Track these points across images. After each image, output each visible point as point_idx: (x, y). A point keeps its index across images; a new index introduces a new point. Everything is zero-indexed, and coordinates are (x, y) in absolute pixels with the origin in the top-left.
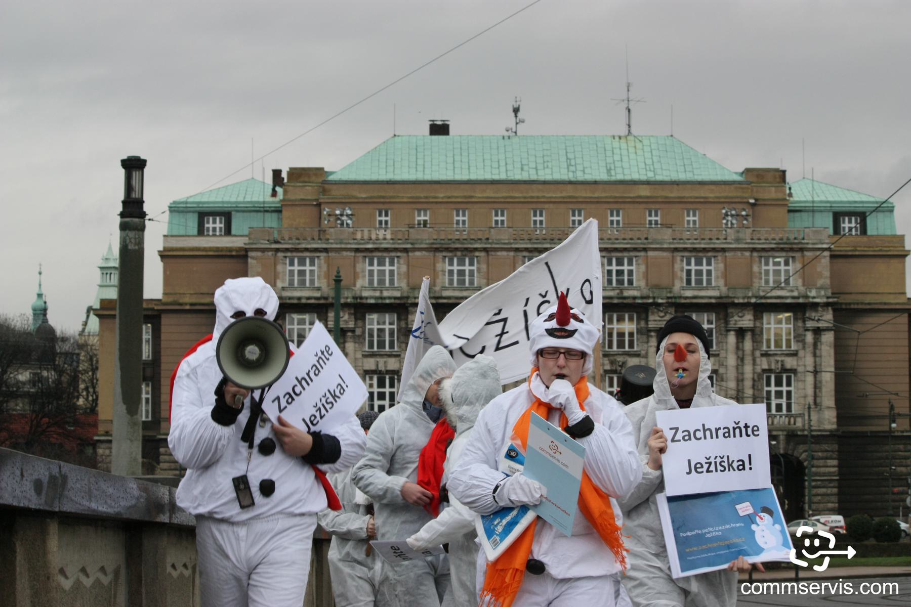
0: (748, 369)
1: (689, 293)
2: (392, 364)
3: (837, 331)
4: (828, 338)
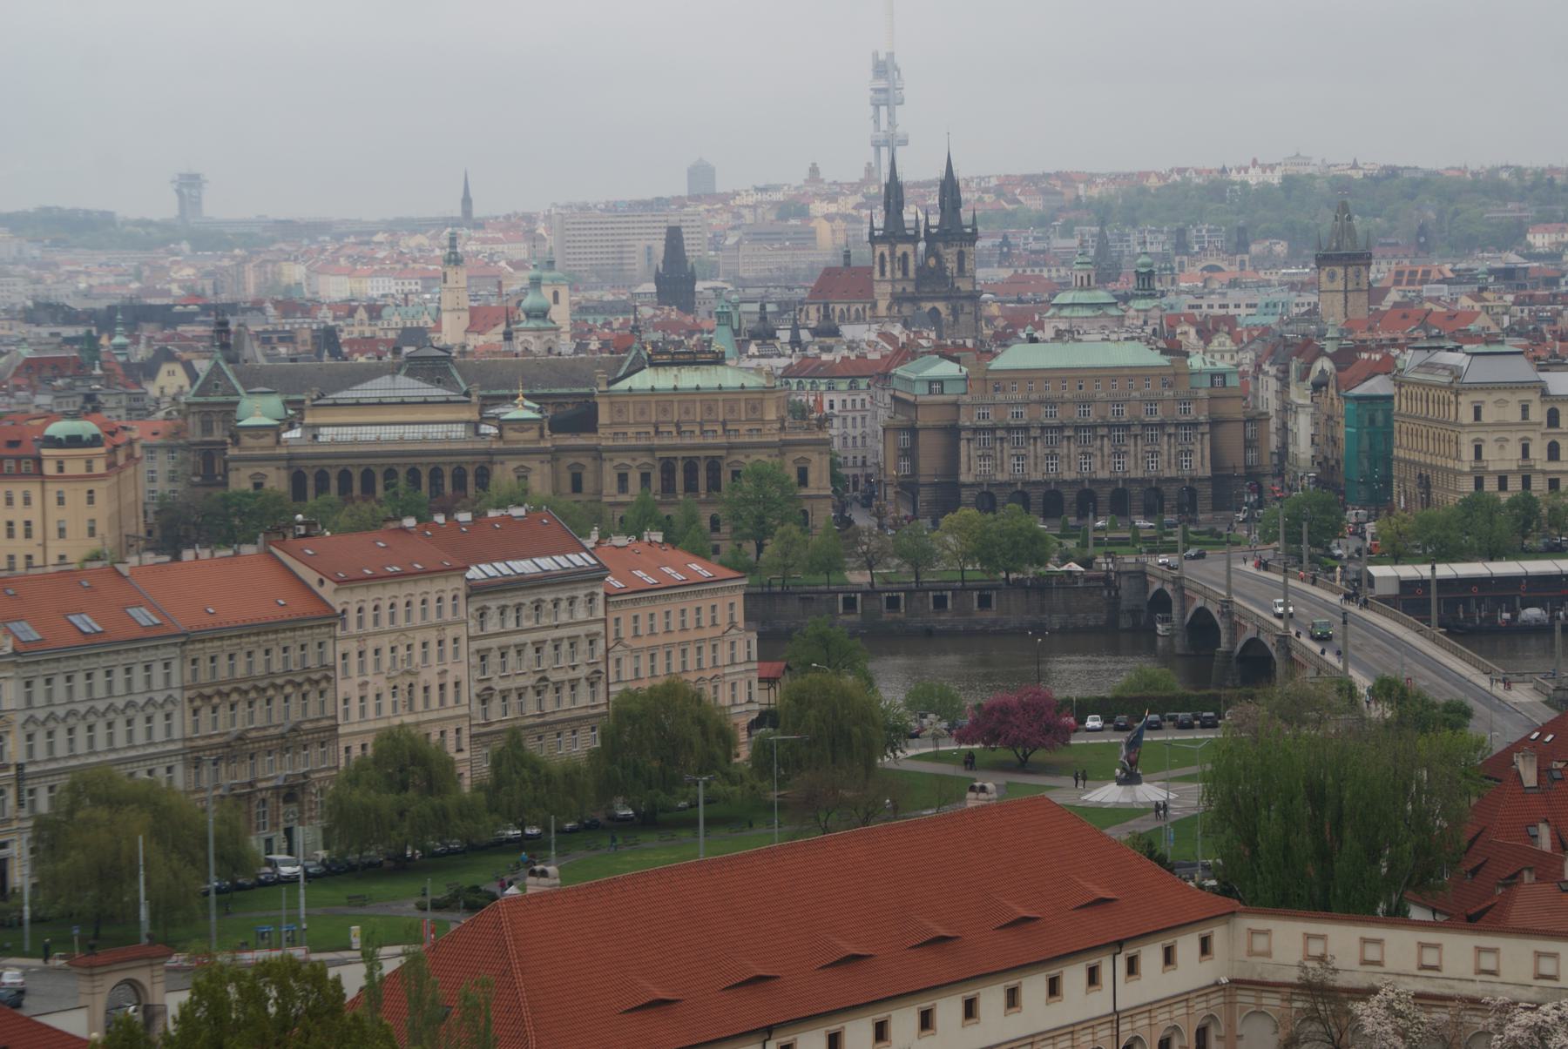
0: (1173, 451)
2: (1023, 452)
3: (1211, 432)
4: (1207, 437)
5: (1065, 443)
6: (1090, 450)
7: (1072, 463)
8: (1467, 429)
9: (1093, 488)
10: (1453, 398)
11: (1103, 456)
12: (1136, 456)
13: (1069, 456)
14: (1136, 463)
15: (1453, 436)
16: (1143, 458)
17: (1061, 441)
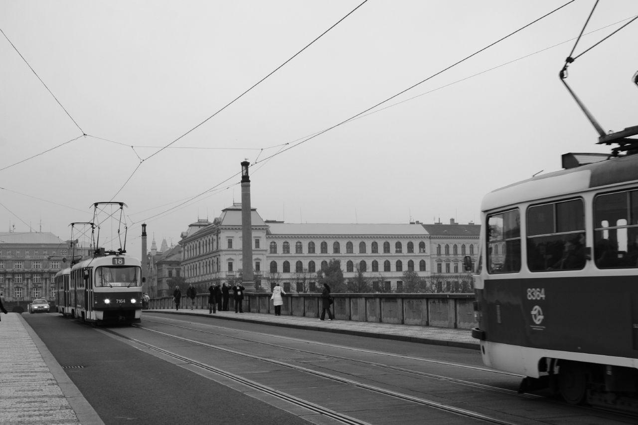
1: (53, 270)
5: (7, 282)
6: (21, 286)
7: (11, 292)
8: (224, 253)
9: (22, 306)
10: (215, 237)
11: (28, 289)
12: (46, 289)
13: (9, 289)
14: (46, 292)
15: (215, 259)
16: (50, 291)
17: (5, 281)
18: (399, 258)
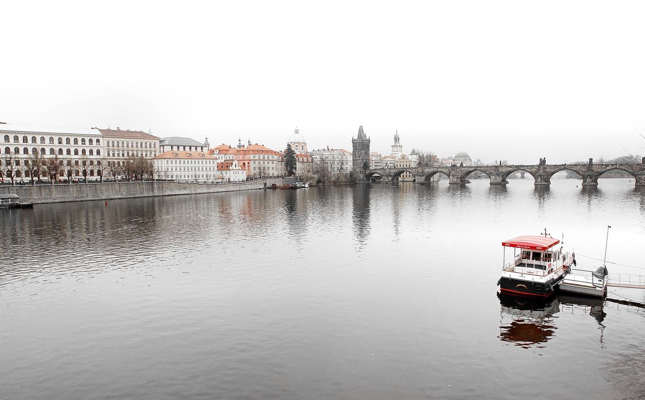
18: (44, 147)
